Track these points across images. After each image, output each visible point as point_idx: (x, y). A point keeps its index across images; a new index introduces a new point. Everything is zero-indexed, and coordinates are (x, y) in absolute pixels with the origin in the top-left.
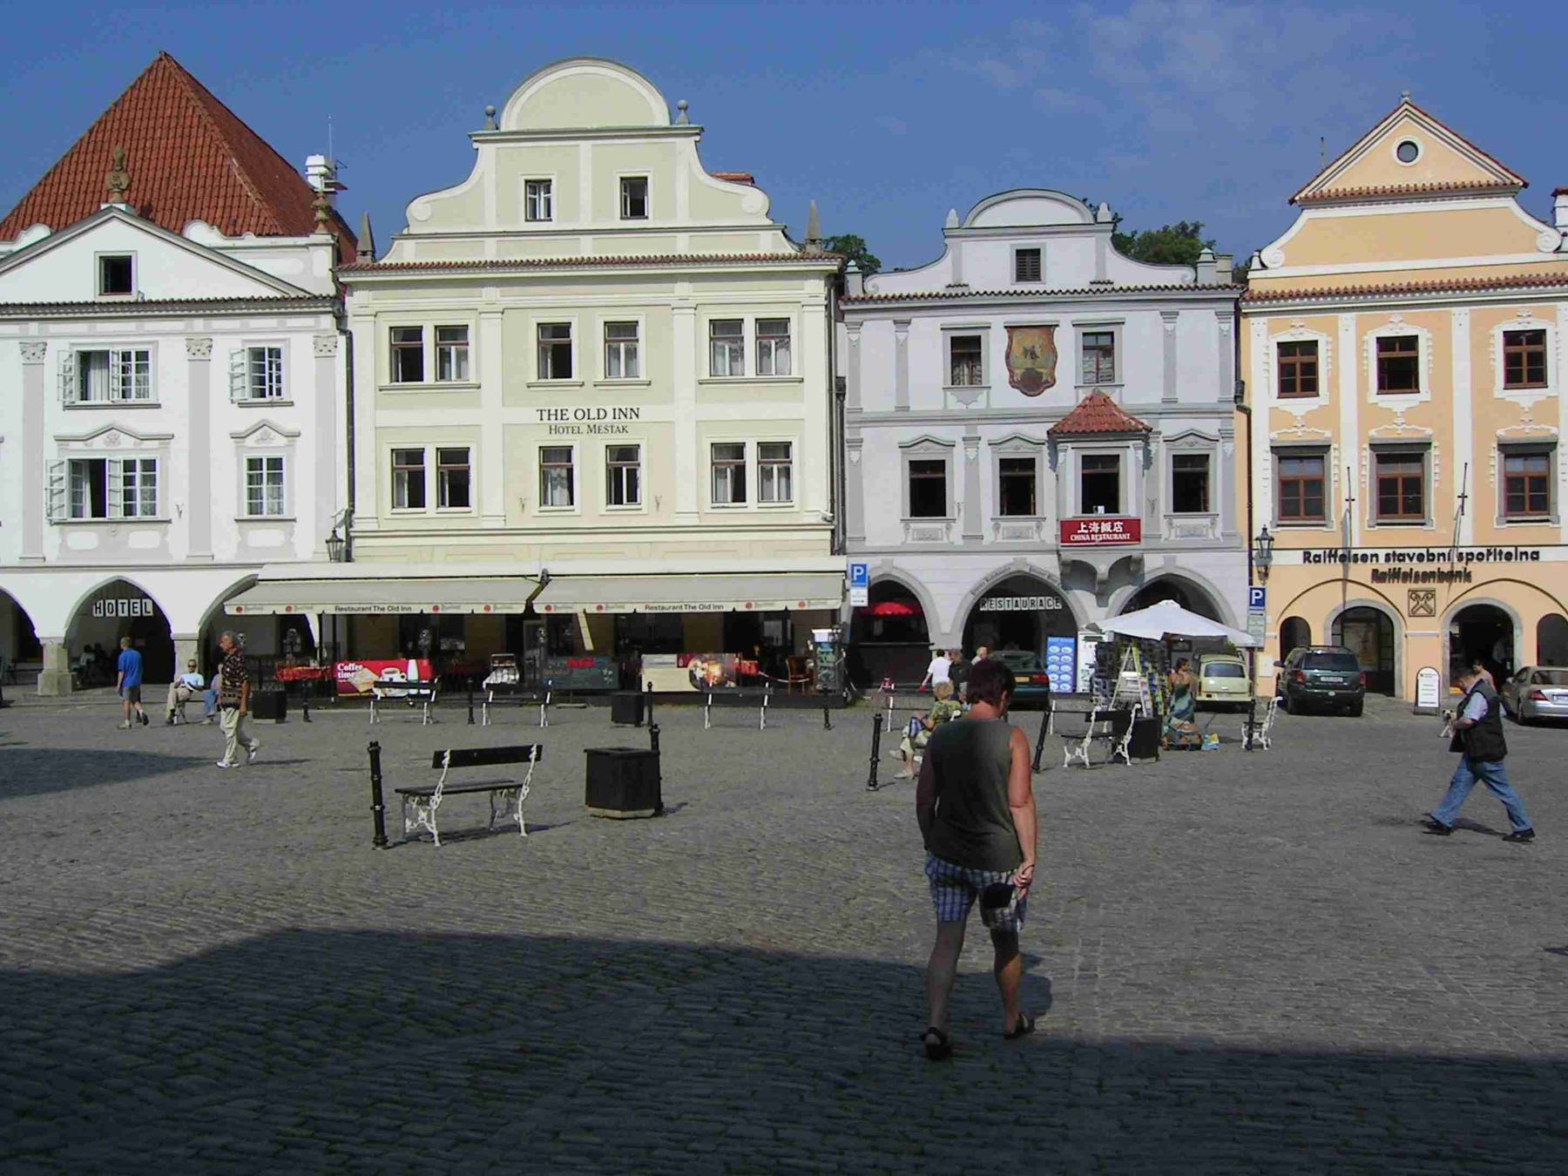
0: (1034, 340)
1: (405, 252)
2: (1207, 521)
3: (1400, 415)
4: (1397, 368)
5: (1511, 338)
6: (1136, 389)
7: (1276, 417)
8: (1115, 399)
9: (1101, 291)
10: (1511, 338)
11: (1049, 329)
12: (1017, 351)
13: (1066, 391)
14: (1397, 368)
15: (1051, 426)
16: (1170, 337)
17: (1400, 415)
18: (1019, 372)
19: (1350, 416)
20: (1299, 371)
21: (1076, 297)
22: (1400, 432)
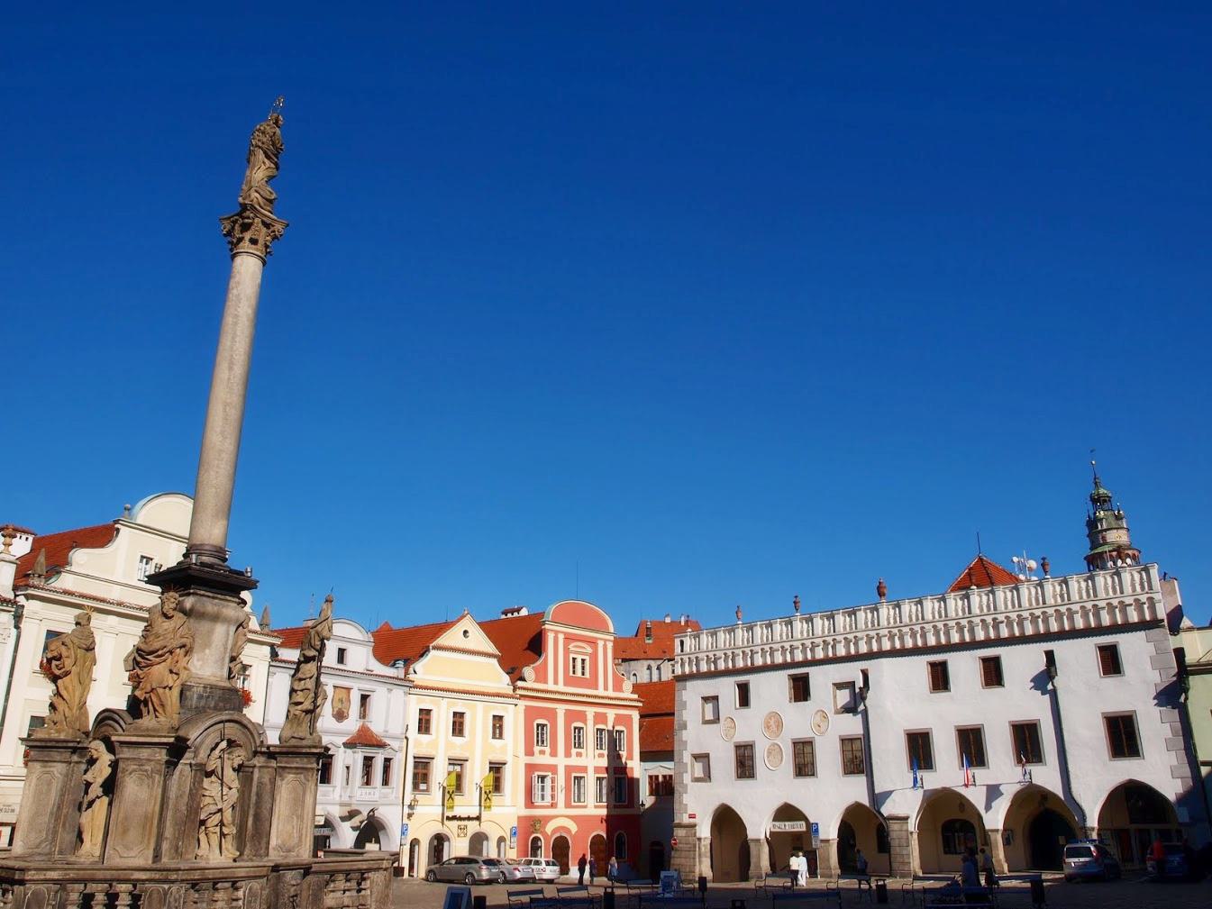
0: (343, 694)
1: (65, 581)
2: (390, 791)
3: (458, 746)
4: (458, 726)
5: (494, 716)
6: (377, 726)
7: (421, 745)
8: (369, 725)
9: (368, 674)
10: (494, 716)
11: (348, 689)
12: (336, 699)
13: (352, 725)
14: (458, 726)
15: (345, 739)
16: (389, 701)
17: (458, 746)
18: (336, 710)
19: (439, 745)
20: (424, 724)
21: (357, 675)
22: (458, 754)
